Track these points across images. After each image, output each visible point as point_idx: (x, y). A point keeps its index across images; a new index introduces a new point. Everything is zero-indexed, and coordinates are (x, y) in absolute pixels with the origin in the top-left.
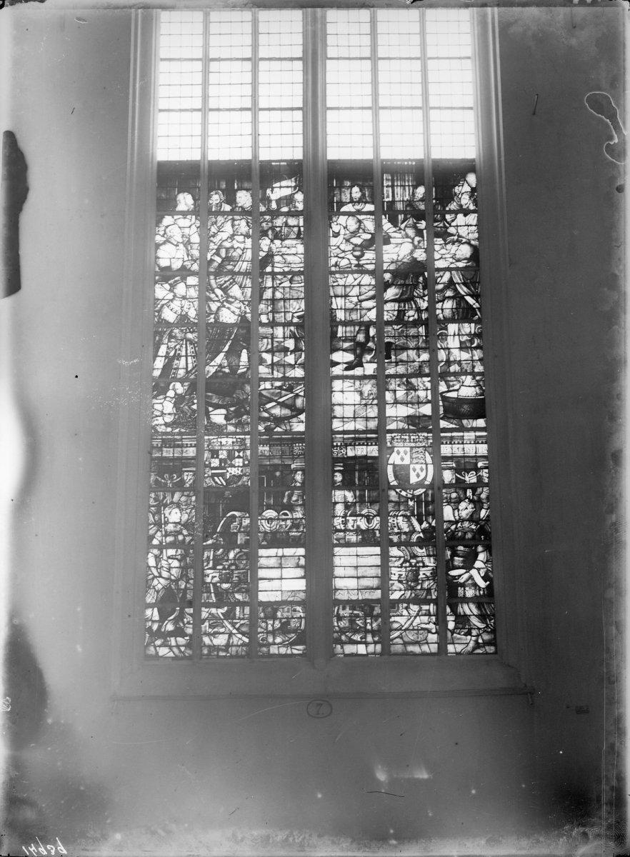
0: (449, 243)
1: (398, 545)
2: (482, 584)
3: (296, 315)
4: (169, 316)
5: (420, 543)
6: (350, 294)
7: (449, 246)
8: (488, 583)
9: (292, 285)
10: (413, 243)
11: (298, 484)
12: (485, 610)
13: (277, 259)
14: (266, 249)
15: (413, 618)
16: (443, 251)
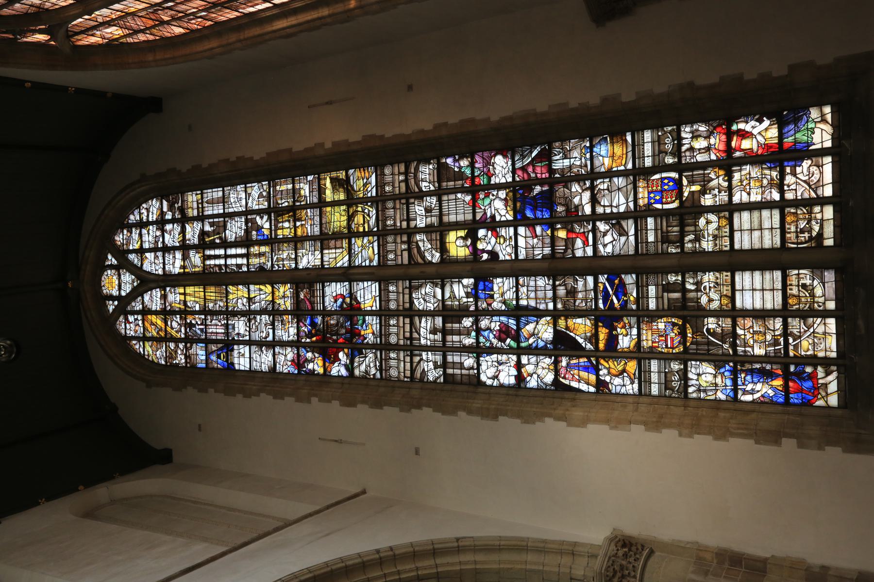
0: (494, 172)
1: (731, 196)
2: (766, 123)
3: (547, 282)
4: (549, 378)
5: (729, 177)
6: (532, 245)
7: (497, 172)
8: (765, 118)
9: (526, 284)
10: (494, 200)
11: (680, 278)
12: (790, 118)
13: (507, 296)
14: (500, 305)
15: (798, 180)
16: (500, 176)
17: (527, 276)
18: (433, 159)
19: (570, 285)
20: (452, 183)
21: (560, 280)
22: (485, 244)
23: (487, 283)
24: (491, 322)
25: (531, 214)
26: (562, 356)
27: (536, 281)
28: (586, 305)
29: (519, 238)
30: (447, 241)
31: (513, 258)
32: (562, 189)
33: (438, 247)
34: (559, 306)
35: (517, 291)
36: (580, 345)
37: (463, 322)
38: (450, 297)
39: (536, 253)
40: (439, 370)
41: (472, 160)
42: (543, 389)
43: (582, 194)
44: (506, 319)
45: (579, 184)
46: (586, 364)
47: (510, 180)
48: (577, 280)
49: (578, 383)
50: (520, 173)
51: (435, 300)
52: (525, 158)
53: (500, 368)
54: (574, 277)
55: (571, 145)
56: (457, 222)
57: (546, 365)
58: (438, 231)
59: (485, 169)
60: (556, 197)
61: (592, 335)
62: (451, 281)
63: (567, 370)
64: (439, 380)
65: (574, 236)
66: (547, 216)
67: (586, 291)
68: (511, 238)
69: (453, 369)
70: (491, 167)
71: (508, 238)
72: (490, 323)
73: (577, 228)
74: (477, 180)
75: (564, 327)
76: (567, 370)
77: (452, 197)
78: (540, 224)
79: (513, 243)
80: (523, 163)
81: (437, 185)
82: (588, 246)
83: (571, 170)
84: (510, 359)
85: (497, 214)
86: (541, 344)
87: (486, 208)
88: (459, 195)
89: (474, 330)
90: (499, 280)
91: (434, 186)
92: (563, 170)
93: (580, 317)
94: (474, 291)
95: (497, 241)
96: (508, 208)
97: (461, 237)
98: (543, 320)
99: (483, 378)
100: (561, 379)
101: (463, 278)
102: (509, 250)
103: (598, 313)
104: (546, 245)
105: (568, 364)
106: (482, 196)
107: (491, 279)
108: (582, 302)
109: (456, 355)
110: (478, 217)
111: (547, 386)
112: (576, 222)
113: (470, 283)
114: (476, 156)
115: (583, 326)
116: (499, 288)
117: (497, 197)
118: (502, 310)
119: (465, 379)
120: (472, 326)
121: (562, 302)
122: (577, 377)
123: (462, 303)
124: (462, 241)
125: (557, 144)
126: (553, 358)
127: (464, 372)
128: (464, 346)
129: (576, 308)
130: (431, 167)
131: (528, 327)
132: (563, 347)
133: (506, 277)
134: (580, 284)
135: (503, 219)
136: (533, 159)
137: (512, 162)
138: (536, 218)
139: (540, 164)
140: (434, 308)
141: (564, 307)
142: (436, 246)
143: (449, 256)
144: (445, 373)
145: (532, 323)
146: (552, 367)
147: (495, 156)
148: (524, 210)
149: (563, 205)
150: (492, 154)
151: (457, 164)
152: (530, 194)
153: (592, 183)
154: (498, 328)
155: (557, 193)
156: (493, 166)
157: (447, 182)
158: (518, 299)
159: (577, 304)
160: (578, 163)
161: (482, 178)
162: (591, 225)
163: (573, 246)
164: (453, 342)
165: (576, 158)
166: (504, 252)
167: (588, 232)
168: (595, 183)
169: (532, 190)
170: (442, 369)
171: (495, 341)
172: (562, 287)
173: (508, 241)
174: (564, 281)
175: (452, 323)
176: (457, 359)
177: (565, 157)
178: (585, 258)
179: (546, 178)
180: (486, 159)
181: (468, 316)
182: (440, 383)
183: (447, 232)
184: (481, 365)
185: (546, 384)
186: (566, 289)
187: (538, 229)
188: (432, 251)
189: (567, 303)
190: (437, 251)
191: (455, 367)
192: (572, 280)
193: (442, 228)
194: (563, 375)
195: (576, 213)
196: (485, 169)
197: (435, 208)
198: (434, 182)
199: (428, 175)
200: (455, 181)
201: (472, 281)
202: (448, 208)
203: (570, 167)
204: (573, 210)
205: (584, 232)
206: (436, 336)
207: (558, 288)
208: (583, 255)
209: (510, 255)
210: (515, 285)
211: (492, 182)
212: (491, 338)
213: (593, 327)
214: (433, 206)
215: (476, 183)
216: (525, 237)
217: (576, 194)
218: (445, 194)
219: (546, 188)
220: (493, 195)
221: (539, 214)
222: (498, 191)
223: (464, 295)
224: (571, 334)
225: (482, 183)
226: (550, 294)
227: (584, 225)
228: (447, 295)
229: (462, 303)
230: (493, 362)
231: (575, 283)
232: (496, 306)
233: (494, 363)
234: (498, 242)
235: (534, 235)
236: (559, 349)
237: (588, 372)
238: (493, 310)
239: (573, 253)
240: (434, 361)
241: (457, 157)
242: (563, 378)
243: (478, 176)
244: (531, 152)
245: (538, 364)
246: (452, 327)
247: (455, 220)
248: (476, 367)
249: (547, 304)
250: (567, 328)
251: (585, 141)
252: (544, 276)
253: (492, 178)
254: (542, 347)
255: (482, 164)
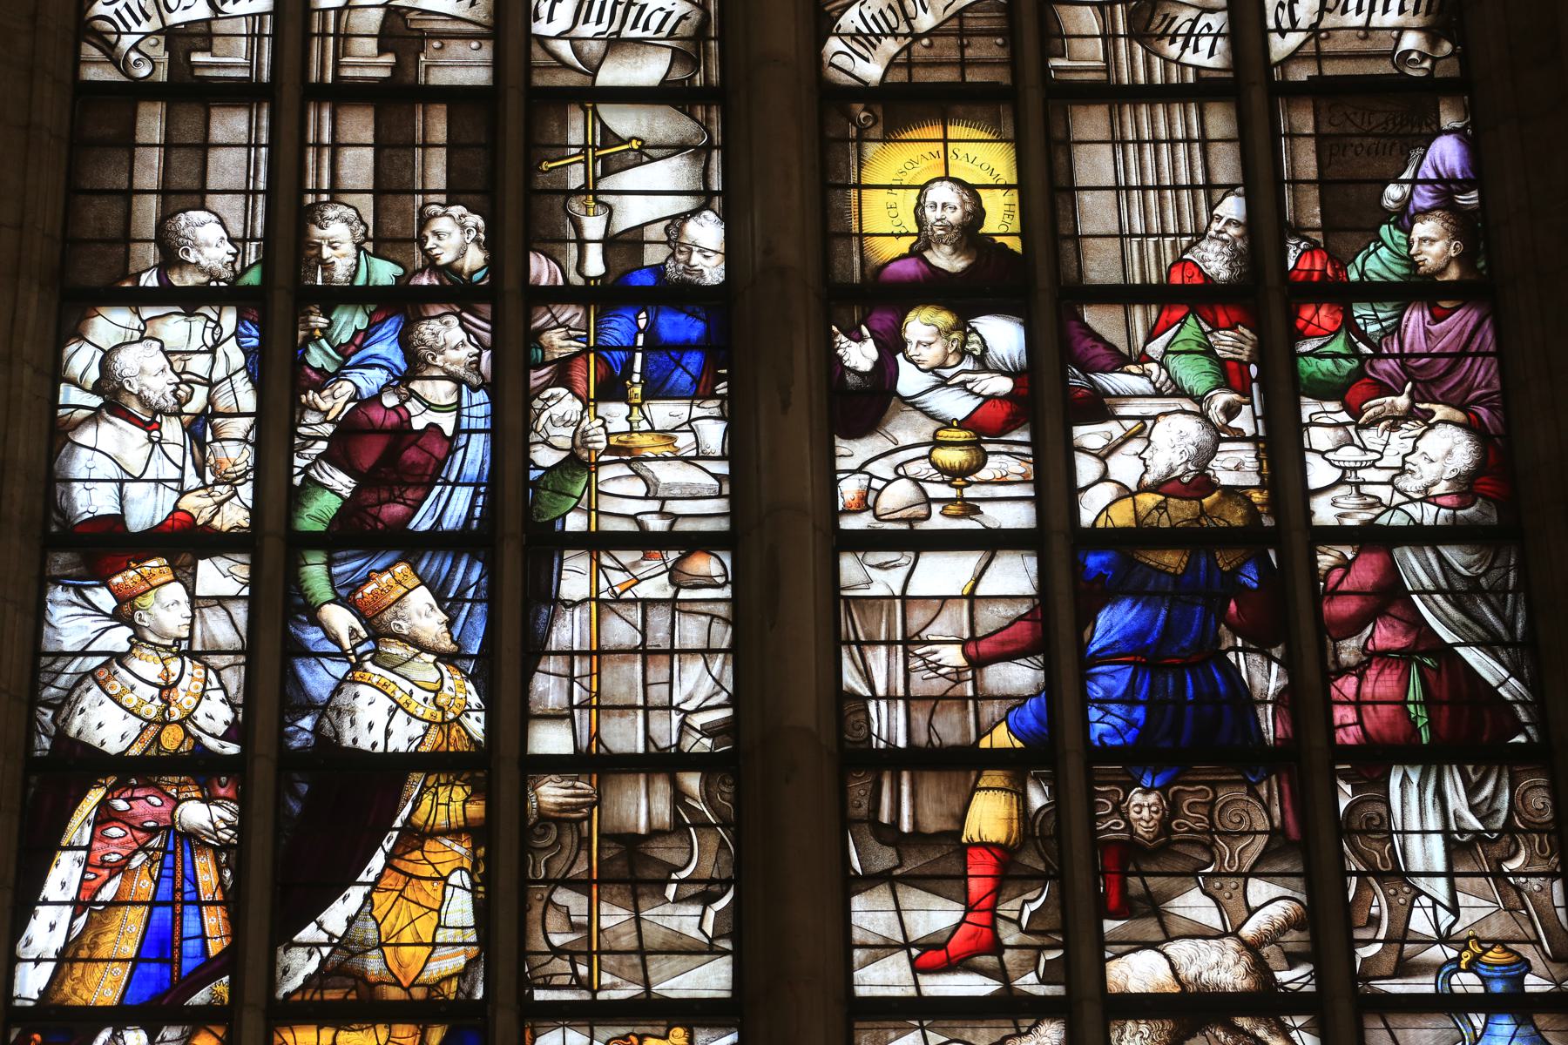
0: (1374, 422)
3: (698, 720)
6: (932, 633)
7: (1371, 437)
9: (683, 594)
10: (1203, 416)
13: (613, 477)
14: (562, 437)
16: (1349, 455)
17: (733, 601)
18: (1459, 55)
19: (676, 858)
20: (1307, 163)
21: (708, 799)
22: (931, 355)
23: (693, 360)
24: (458, 381)
25: (1114, 635)
26: (242, 800)
27: (707, 652)
28: (557, 952)
29: (968, 562)
30: (955, 131)
31: (850, 523)
32: (1262, 824)
33: (921, 75)
34: (551, 793)
35: (643, 541)
36: (312, 910)
37: (457, 210)
38: (609, 137)
39: (878, 659)
40: (160, 53)
41: (1450, 290)
42: (35, 686)
43: (1231, 943)
44: (472, 471)
45: (1289, 924)
46: (191, 947)
47: (1324, 512)
48: (706, 899)
49: (71, 893)
50: (1365, 573)
51: (596, 48)
52: (1458, 606)
53: (172, 430)
54: (725, 884)
55: (1534, 884)
56: (1072, 190)
57: (188, 702)
58: (1015, 75)
59: (1388, 365)
60: (1214, 785)
61: (372, 986)
62: (708, 148)
63: (153, 832)
64: (95, 53)
65: (975, 886)
66: (1101, 725)
67: (642, 952)
68: (970, 508)
69: (168, 146)
70: (1402, 401)
71: (969, 493)
72: (450, 376)
73: (1026, 905)
74: (1325, 317)
75: (420, 817)
76: (153, 832)
77: (1226, 167)
78: (1050, 687)
79: (938, 522)
80: (1422, 592)
81: (1301, 73)
82: (917, 968)
83: (1381, 877)
84: (224, 490)
85: (1115, 429)
86: (319, 679)
87: (1153, 367)
88: (1232, 207)
89: (409, 273)
90: (713, 434)
91: (1294, 56)
92: (1383, 829)
93: (482, 911)
94: (648, 280)
95: (947, 424)
96: (1149, 500)
97: (977, 215)
98: (462, 692)
99: (109, 325)
100: (95, 796)
101: (726, 218)
102: (897, 496)
103: (504, 1020)
104: (921, 718)
105: (191, 839)
106: (1225, 342)
107: (722, 388)
108: (574, 928)
109: (251, 167)
110: (1101, 319)
111: (57, 709)
112: (1063, 901)
113: (696, 259)
114: (1473, 317)
115: (425, 927)
116: (667, 435)
117: (1220, 434)
118: (526, 447)
119: (98, 216)
120: (431, 263)
121: (576, 808)
122: (107, 894)
123: (575, 206)
124: (954, 217)
125: (1539, 800)
126: (232, 749)
127: (147, 210)
128: (309, 216)
129: (539, 893)
130: (1411, 41)
131: (422, 598)
132: (296, 807)
133: (732, 478)
134: (687, 921)
135: (1086, 469)
136: (1447, 653)
137: (1435, 528)
138: (1086, 663)
139: (1415, 691)
140: (542, 40)
141: (545, 818)
142: (928, 64)
143: (861, 139)
144: (146, 91)
145: (450, 624)
146: (172, 739)
147: (1471, 426)
148: (1138, 595)
149: (1164, 826)
150: (1483, 412)
151: (1423, 197)
152: (1236, 632)
153: (1295, 1002)
154: (418, 424)
155: (1241, 792)
156: (1410, 414)
157: (1318, 136)
158: (596, 543)
159: (563, 897)
160: (1420, 922)
161: (1338, 345)
162: (1043, 990)
163: (914, 881)
164: (336, 146)
165: (1454, 909)
166: (883, 469)
167: (1001, 973)
168: (1299, 1021)
169: (1260, 645)
170: (162, 75)
171: (336, 400)
172: (663, 810)
173: (951, 493)
174: (701, 824)
175: (452, 146)
176: (227, 167)
177: (1454, 849)
178: (843, 944)
179: (1331, 728)
180: (1450, 371)
181: (491, 243)
182: (78, 62)
183: (1009, 131)
184: (189, 313)
185: (66, 703)
186: (654, 833)
187: (1019, 676)
188: (894, 34)
189: (567, 840)
190: (892, 64)
191: (176, 156)
192: (708, 871)
193: (1033, 98)
194: (121, 805)
195: (1113, 902)
196: (1388, 365)
197: (1157, 61)
198: (1319, 57)
199: (1360, 20)
200: (1322, 182)
201: (712, 271)
202: (1156, 142)
203: (1398, 875)
204: (1134, 882)
205: (997, 948)
206: (371, 45)
207: (662, 788)
208: (857, 936)
209: (865, 503)
210: (684, 526)
211: (1309, 408)
212: (356, 376)
213: (418, 993)
214: (1173, 50)
215: (1307, 313)
216: (972, 597)
217: (1234, 905)
218: (1243, 123)
219: (1269, 724)
220: (1231, 411)
221: (1109, 681)
222: (1254, 439)
223: (623, 222)
224: (377, 862)
225: (1307, 347)
226: (625, 736)
227: (1041, 949)
228: (625, 122)
229: (575, 206)
230: (210, 384)
231: (692, 890)
232: (557, 410)
233: (201, 393)
234: (945, 435)
235: (984, 647)
236: (283, 786)
237: (137, 961)
238: (529, 395)
239: (870, 881)
240: (219, 27)
241: (1470, 199)
242: (103, 804)
243: (1349, 324)
244: (1489, 645)
245: (194, 655)
246: (426, 145)
247: (1083, 176)
248: (176, 280)
249: (563, 716)
250: (415, 836)
251: (1556, 969)
252: (733, 701)
253: (1331, 406)
254: (299, 683)
255: (1421, 347)
